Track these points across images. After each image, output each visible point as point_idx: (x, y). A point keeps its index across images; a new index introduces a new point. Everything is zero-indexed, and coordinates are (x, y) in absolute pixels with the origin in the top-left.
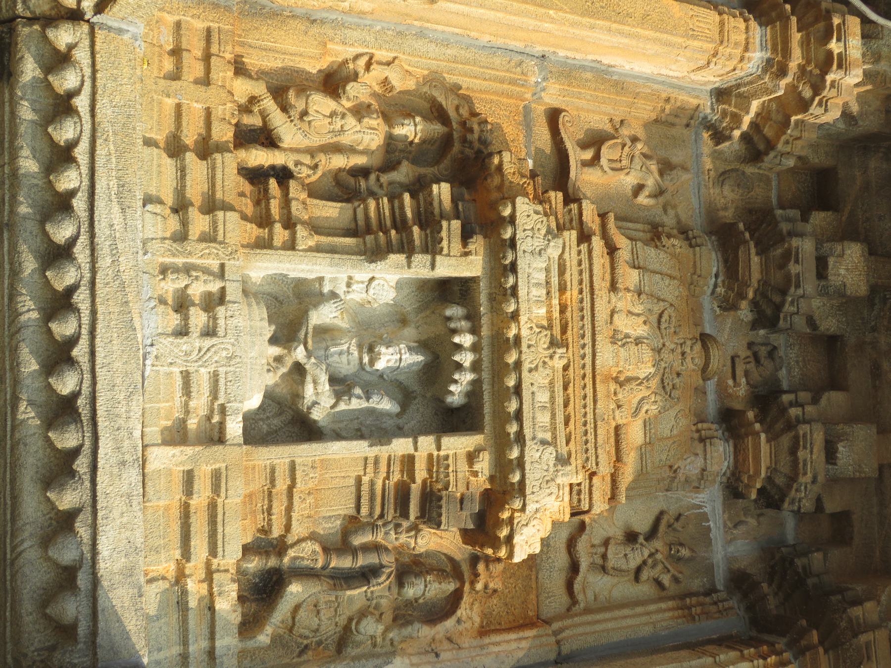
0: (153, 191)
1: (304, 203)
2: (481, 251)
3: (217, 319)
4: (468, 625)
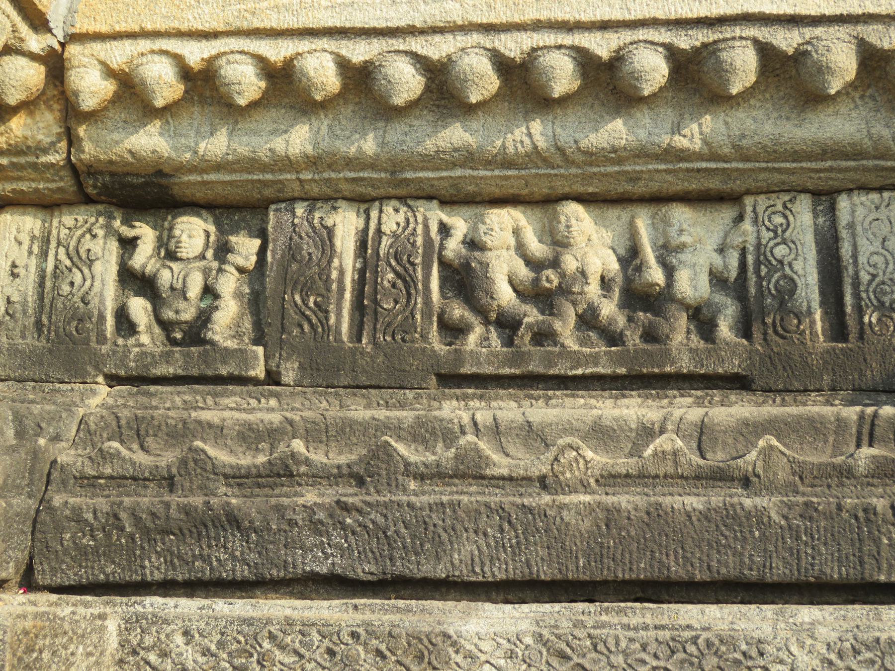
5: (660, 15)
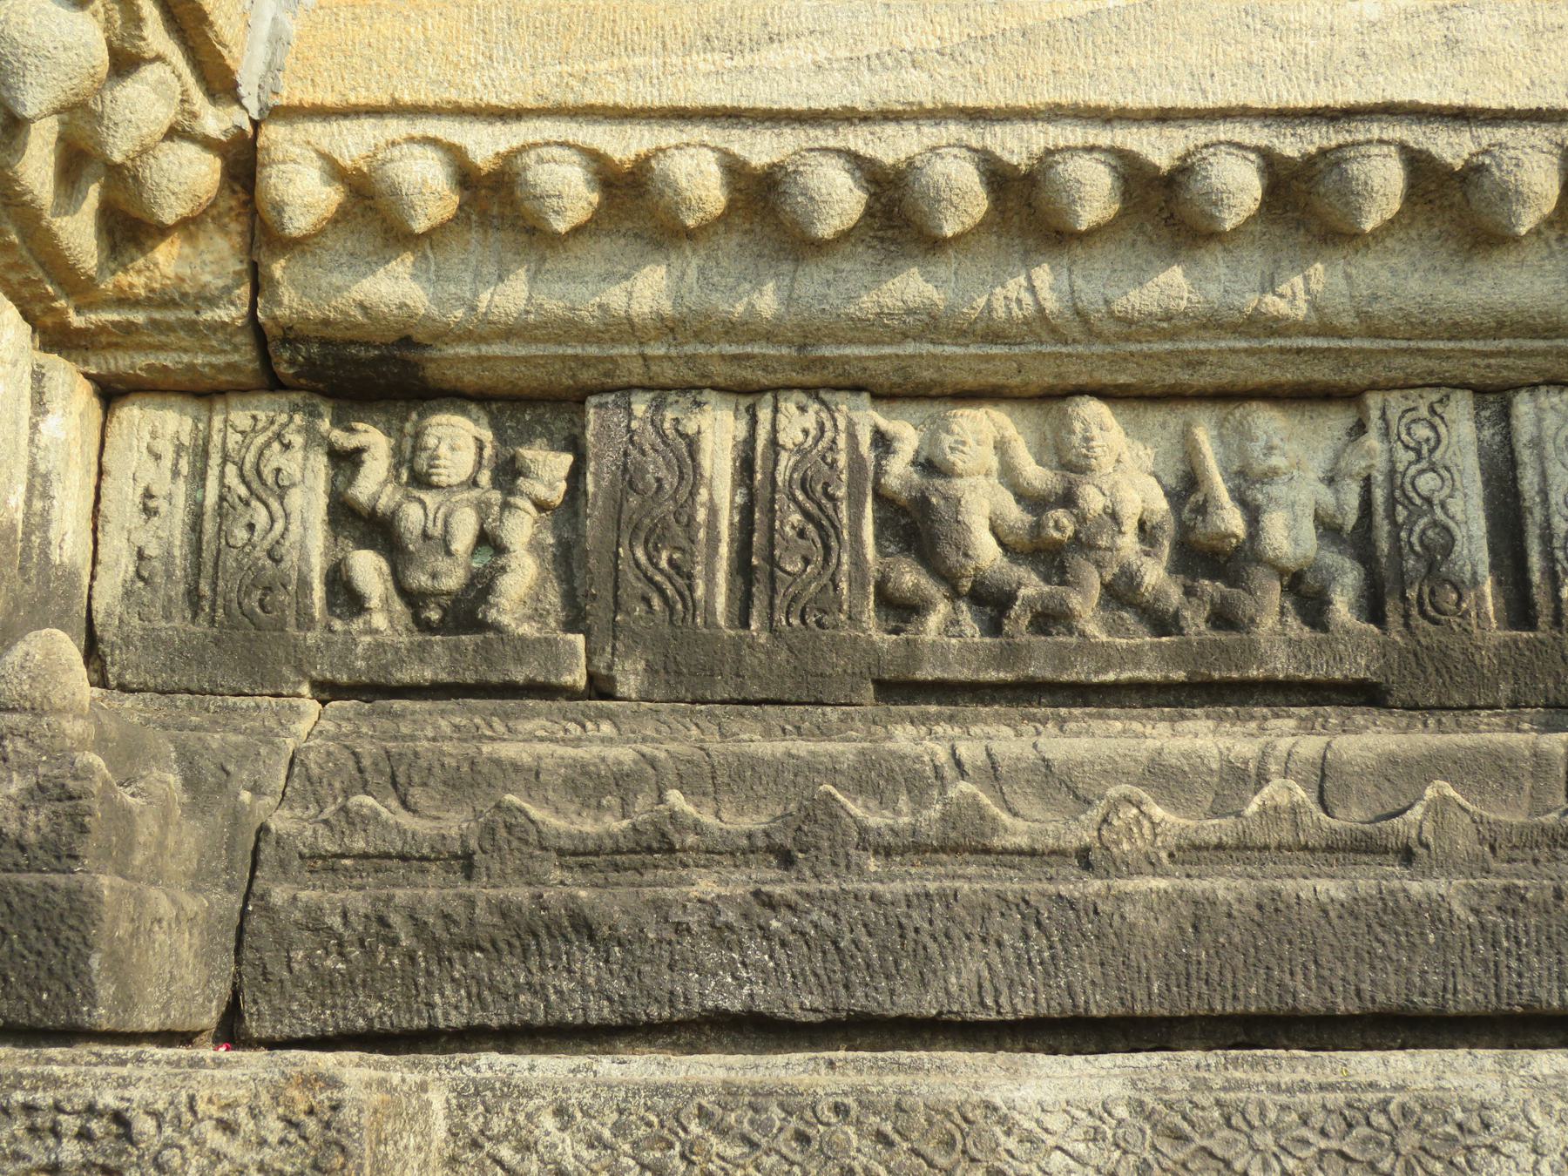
5: (1255, 101)
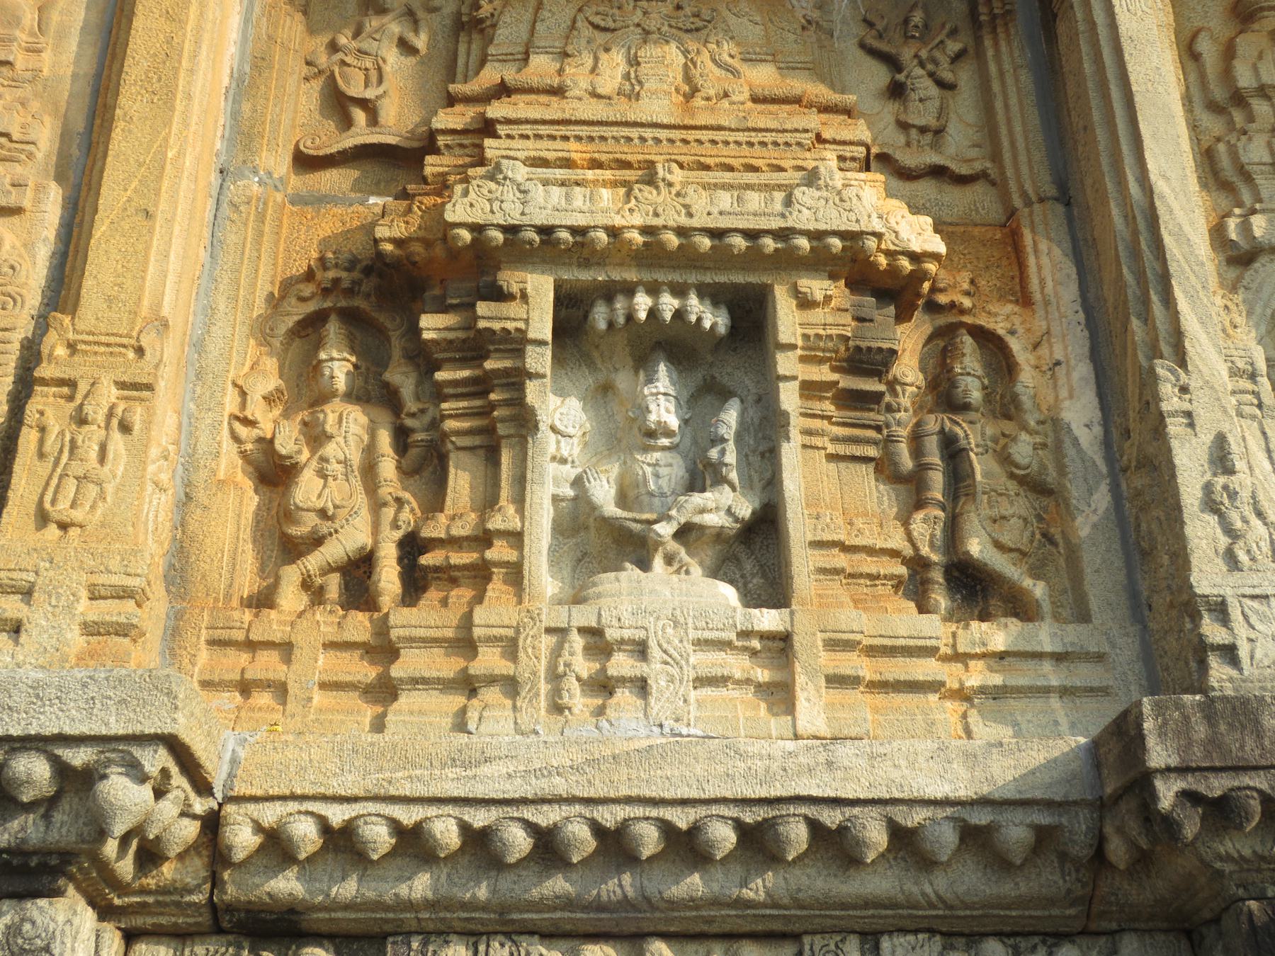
0: (447, 722)
1: (453, 518)
2: (519, 275)
3: (622, 639)
4: (1017, 320)
5: (729, 795)
